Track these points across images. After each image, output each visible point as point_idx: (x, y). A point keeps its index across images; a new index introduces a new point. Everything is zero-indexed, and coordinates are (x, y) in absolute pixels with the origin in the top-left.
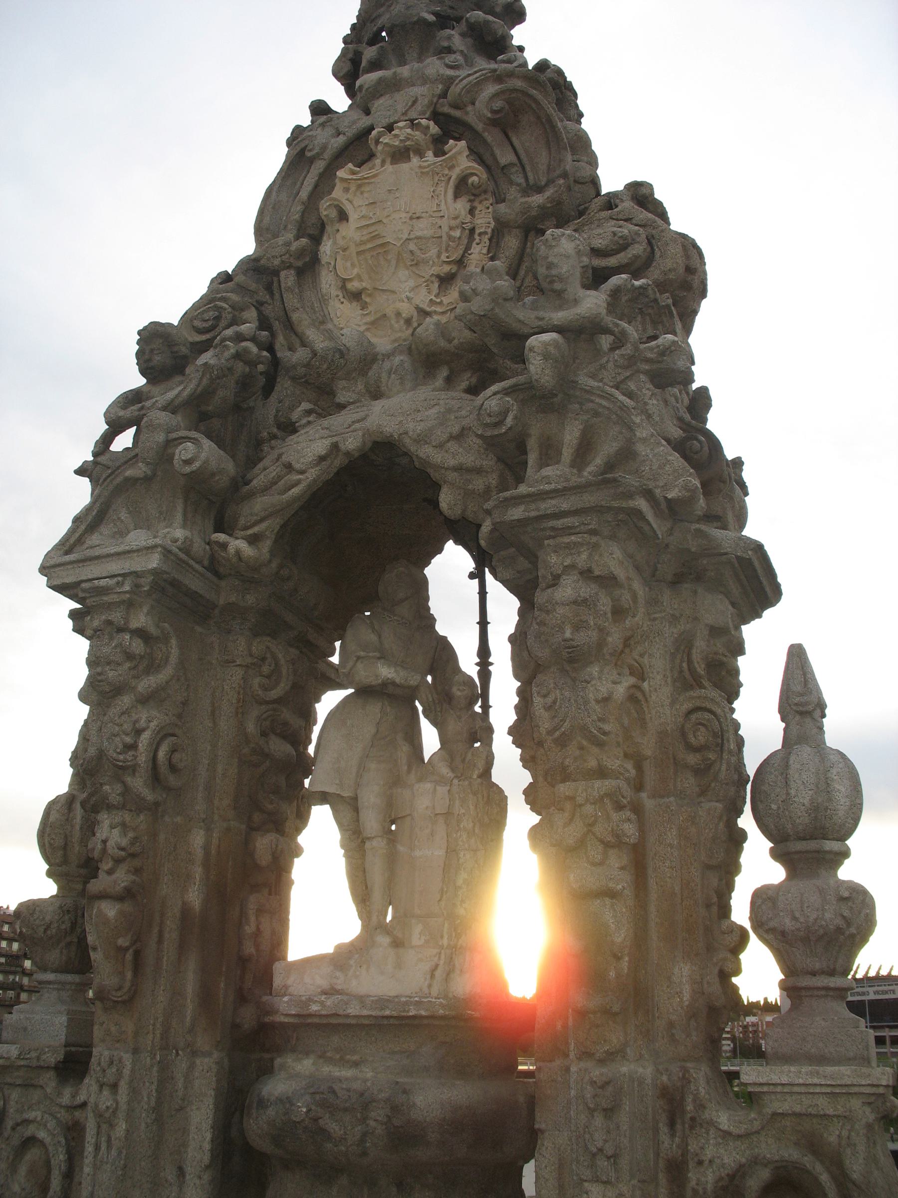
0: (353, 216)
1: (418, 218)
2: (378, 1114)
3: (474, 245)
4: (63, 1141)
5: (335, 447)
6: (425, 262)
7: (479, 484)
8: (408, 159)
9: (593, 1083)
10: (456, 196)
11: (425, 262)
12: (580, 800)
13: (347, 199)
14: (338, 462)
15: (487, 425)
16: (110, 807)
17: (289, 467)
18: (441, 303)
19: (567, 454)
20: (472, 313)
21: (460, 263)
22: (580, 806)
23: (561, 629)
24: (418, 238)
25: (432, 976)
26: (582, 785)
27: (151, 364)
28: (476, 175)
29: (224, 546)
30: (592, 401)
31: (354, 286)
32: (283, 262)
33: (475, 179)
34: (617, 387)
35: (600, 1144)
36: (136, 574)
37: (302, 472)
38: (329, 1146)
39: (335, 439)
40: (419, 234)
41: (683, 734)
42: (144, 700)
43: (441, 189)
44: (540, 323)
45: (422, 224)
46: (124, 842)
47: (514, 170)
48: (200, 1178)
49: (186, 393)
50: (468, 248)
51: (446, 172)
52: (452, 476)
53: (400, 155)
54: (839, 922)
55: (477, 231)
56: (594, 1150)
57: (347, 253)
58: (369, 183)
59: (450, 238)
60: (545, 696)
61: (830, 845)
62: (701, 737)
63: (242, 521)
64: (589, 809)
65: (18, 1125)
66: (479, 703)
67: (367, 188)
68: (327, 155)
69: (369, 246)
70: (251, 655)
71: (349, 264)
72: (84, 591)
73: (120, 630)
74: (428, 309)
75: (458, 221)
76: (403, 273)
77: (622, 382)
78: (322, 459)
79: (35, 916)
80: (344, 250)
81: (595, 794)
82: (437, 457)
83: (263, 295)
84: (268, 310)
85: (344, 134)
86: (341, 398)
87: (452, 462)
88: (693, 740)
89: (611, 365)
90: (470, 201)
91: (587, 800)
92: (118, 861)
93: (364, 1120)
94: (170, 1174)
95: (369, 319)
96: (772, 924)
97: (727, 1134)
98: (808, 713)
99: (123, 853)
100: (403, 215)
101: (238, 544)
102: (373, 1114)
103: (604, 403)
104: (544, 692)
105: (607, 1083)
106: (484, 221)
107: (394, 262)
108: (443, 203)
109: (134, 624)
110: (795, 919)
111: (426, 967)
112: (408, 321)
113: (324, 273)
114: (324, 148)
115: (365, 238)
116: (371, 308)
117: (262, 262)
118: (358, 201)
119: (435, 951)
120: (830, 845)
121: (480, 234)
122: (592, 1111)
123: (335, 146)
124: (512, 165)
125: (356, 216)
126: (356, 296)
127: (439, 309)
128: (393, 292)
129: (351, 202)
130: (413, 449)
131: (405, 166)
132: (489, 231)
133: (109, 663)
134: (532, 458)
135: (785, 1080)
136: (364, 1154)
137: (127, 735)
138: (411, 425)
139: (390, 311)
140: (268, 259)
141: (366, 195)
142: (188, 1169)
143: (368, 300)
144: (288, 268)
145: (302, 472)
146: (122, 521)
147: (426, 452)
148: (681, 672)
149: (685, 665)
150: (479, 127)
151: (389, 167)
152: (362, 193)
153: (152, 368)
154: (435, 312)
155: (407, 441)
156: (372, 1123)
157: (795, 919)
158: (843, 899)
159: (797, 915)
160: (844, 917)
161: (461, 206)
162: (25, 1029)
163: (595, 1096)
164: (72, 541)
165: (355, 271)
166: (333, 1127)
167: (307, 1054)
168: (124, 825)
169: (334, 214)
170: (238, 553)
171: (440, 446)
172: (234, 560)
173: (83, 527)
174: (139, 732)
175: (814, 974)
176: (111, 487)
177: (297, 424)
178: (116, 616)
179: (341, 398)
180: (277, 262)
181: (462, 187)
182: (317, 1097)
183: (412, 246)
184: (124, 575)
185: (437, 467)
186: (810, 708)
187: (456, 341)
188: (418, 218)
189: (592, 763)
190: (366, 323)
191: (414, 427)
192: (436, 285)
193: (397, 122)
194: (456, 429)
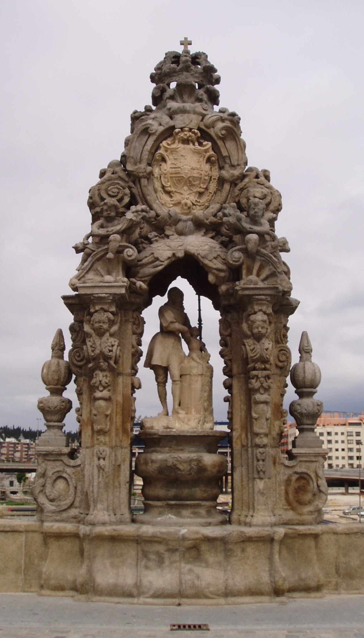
0: (169, 162)
1: (193, 169)
2: (195, 463)
3: (211, 182)
4: (74, 477)
5: (174, 254)
6: (194, 185)
7: (222, 274)
8: (189, 144)
9: (260, 453)
10: (207, 162)
11: (194, 185)
12: (260, 376)
13: (167, 155)
14: (173, 259)
15: (234, 261)
16: (102, 370)
17: (157, 259)
18: (199, 202)
19: (255, 271)
20: (229, 222)
21: (207, 189)
22: (259, 378)
23: (258, 328)
24: (193, 177)
25: (199, 423)
26: (260, 372)
27: (110, 215)
28: (213, 157)
29: (135, 284)
30: (264, 257)
31: (169, 189)
32: (143, 175)
33: (213, 158)
34: (271, 253)
35: (261, 468)
36: (115, 294)
37: (163, 262)
38: (179, 472)
39: (174, 252)
40: (194, 175)
41: (278, 357)
42: (112, 335)
43: (201, 159)
44: (251, 230)
45: (196, 171)
46: (107, 381)
47: (227, 158)
48: (125, 485)
49: (123, 228)
50: (209, 183)
51: (204, 154)
52: (214, 271)
53: (186, 141)
54: (317, 411)
55: (213, 178)
56: (260, 470)
57: (166, 176)
58: (175, 151)
59: (205, 180)
60: (250, 346)
61: (313, 390)
62: (283, 358)
63: (140, 275)
64: (262, 379)
65: (55, 472)
66: (199, 337)
67: (174, 153)
68: (157, 134)
69: (174, 175)
70: (133, 318)
71: (166, 180)
72: (94, 297)
73: (106, 311)
74: (195, 203)
75: (207, 173)
76: (186, 188)
77: (273, 252)
78: (169, 258)
79: (50, 403)
80: (165, 174)
81: (264, 375)
82: (211, 264)
83: (131, 184)
84: (135, 191)
85: (164, 126)
86: (168, 232)
87: (214, 267)
88: (281, 359)
89: (270, 246)
90: (211, 165)
91: (262, 377)
92: (105, 388)
93: (190, 465)
94: (117, 484)
95: (173, 202)
96: (299, 411)
97: (287, 467)
98: (308, 352)
99: (107, 385)
100: (189, 167)
101: (139, 283)
102: (193, 463)
103: (268, 259)
104: (250, 345)
105: (264, 453)
106: (215, 173)
107: (183, 183)
108: (202, 165)
109: (111, 310)
110: (306, 410)
111: (197, 421)
112: (189, 208)
113: (155, 180)
114: (156, 131)
115: (173, 172)
116: (173, 199)
117: (134, 173)
118: (171, 157)
119: (200, 416)
120: (313, 390)
121: (214, 179)
122: (258, 460)
123: (160, 130)
124: (226, 156)
125: (170, 163)
126: (168, 193)
127: (199, 204)
128: (182, 194)
129: (168, 157)
130: (202, 260)
131: (187, 146)
132: (217, 178)
133: (104, 323)
134: (244, 272)
135: (304, 452)
136: (191, 474)
137: (109, 346)
138: (200, 252)
139: (183, 202)
140: (137, 173)
141: (174, 155)
142: (121, 483)
143: (172, 195)
144: (145, 178)
145: (163, 262)
146: (98, 271)
147: (206, 262)
148: (278, 338)
149: (279, 337)
150: (215, 138)
151: (181, 146)
152: (172, 154)
153: (111, 217)
154: (197, 205)
155: (199, 256)
156: (193, 466)
157: (306, 410)
158: (318, 405)
159: (307, 409)
160: (318, 410)
161: (207, 167)
162: (49, 442)
163: (261, 456)
164: (81, 276)
165: (169, 184)
166: (181, 467)
167: (165, 447)
168: (106, 376)
169: (160, 159)
170: (141, 286)
171: (210, 261)
172: (139, 289)
173: (85, 272)
174: (113, 346)
175: (308, 425)
176: (95, 258)
177: (152, 240)
178: (106, 307)
179: (168, 232)
180: (141, 175)
181: (209, 160)
182: (175, 459)
183: (191, 179)
184: (110, 294)
185: (209, 267)
186: (309, 351)
187: (209, 220)
188: (193, 169)
189: (263, 366)
190: (172, 204)
191: (203, 253)
192: (198, 195)
193: (184, 127)
194: (216, 255)
